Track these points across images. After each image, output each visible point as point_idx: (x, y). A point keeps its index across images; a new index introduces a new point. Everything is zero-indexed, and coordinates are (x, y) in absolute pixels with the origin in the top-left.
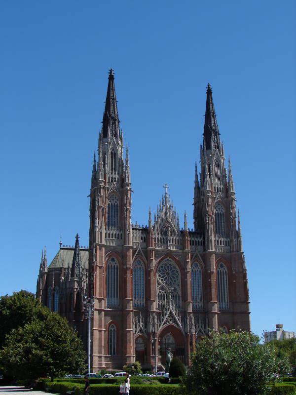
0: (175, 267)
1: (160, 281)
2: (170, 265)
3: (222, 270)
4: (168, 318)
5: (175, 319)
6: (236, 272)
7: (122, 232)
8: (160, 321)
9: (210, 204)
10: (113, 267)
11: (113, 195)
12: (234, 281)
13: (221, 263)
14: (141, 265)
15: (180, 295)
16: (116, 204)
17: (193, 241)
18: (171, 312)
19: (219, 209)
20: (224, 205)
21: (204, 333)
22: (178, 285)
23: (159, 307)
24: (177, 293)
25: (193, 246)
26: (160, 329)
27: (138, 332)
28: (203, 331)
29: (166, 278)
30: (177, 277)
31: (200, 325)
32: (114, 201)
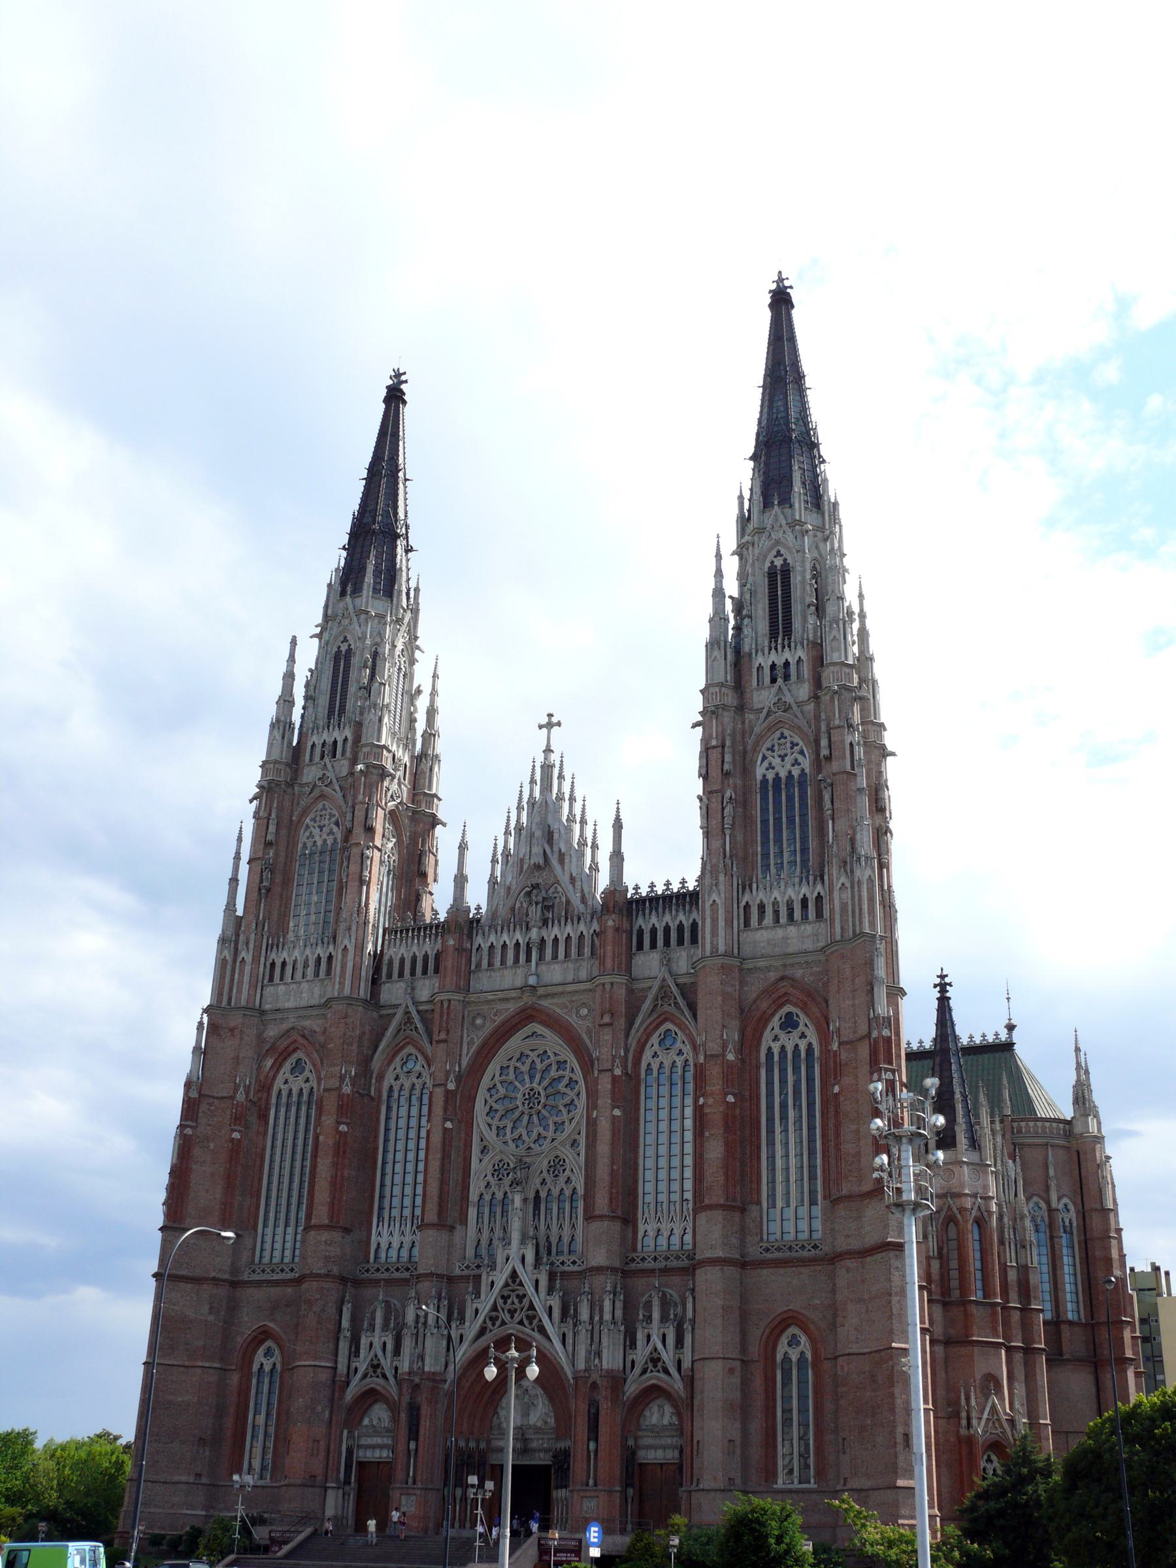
0: (561, 1064)
1: (491, 1136)
3: (789, 1041)
4: (500, 1301)
5: (532, 1307)
6: (840, 1044)
7: (331, 947)
8: (462, 1320)
9: (714, 743)
11: (324, 808)
12: (836, 1089)
13: (788, 1008)
14: (419, 1076)
15: (581, 1191)
16: (330, 842)
17: (654, 931)
18: (514, 1275)
19: (783, 757)
20: (803, 736)
21: (673, 1371)
22: (574, 1143)
23: (477, 1255)
24: (568, 1180)
27: (365, 1376)
28: (668, 1357)
29: (523, 1113)
31: (655, 1330)
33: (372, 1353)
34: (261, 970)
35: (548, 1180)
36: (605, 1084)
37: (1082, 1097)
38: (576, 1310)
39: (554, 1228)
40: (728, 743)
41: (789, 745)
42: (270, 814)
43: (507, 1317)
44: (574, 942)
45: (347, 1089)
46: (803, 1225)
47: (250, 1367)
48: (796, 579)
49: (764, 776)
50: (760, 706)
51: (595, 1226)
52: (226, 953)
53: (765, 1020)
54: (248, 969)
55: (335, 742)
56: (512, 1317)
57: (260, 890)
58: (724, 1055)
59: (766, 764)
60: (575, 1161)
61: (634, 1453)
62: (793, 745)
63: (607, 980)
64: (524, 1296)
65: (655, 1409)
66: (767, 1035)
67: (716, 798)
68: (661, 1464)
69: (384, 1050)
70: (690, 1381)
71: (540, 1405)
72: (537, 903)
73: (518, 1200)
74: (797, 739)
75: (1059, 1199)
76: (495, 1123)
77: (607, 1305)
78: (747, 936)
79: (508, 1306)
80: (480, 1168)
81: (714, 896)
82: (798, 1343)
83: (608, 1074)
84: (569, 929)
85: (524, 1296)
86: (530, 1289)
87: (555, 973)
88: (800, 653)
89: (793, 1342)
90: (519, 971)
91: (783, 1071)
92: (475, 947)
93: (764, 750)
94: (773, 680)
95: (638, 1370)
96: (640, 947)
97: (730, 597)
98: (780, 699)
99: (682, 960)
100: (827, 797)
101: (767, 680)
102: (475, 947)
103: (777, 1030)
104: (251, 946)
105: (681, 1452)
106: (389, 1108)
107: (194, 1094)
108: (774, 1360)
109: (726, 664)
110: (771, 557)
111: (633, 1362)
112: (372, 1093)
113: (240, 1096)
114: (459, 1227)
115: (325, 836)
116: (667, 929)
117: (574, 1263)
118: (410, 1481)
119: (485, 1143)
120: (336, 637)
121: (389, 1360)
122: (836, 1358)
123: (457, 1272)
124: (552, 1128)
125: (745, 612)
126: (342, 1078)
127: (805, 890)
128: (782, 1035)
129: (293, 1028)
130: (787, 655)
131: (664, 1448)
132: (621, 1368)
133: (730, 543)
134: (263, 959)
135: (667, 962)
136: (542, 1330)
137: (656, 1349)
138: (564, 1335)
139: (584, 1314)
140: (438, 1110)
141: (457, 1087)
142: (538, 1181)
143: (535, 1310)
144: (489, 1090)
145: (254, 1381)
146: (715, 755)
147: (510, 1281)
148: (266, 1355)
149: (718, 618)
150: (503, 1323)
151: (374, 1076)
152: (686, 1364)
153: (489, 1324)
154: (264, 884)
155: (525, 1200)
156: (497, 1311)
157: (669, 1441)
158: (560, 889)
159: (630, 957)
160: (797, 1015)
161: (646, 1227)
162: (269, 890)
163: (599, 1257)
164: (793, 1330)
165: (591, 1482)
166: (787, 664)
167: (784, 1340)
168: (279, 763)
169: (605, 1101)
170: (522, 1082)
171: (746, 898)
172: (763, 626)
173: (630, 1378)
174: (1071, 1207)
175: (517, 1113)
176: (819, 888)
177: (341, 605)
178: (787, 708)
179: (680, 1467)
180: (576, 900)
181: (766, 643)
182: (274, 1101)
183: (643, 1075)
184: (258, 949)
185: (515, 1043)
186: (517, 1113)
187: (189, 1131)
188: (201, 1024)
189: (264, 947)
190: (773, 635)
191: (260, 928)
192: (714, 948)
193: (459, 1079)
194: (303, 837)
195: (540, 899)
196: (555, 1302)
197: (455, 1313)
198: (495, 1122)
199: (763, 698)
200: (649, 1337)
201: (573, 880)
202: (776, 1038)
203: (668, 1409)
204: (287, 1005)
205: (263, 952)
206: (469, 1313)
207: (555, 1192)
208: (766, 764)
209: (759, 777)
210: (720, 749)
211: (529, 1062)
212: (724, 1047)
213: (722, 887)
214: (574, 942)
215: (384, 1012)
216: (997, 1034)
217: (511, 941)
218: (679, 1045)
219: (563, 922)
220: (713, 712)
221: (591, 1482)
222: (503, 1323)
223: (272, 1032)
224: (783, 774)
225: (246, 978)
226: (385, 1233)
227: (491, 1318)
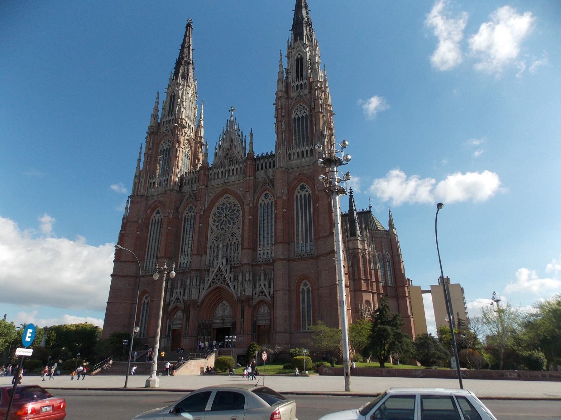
0: (235, 206)
2: (230, 203)
3: (303, 193)
4: (216, 277)
5: (225, 278)
6: (318, 191)
7: (168, 177)
8: (204, 283)
9: (279, 107)
10: (157, 221)
13: (302, 183)
15: (240, 242)
18: (220, 268)
20: (307, 104)
21: (267, 295)
22: (239, 228)
24: (237, 239)
25: (262, 171)
26: (203, 294)
27: (175, 302)
28: (266, 291)
30: (237, 217)
32: (167, 145)
33: (177, 295)
34: (147, 185)
35: (231, 239)
36: (247, 208)
37: (391, 224)
38: (238, 278)
39: (233, 254)
40: (283, 107)
41: (302, 108)
42: (150, 141)
43: (217, 281)
44: (239, 170)
45: (171, 216)
46: (308, 248)
47: (141, 302)
48: (304, 61)
49: (295, 117)
50: (292, 97)
51: (244, 251)
52: (136, 180)
53: (295, 188)
54: (143, 184)
55: (170, 120)
56: (219, 281)
57: (147, 162)
58: (282, 197)
59: (295, 114)
60: (239, 233)
61: (256, 322)
62: (303, 107)
63: (247, 178)
64: (223, 274)
65: (263, 308)
66: (296, 192)
67: (280, 124)
68: (265, 325)
69: (183, 205)
70: (273, 298)
71: (228, 309)
72: (228, 159)
73: (221, 246)
74: (305, 106)
75: (386, 252)
76: (215, 224)
77: (247, 275)
78: (290, 162)
79: (218, 278)
80: (210, 237)
81: (279, 151)
82: (307, 285)
83: (248, 206)
84: (237, 166)
85: (223, 274)
86: (224, 272)
87: (233, 179)
88: (306, 81)
89: (305, 284)
90: (223, 179)
91: (301, 202)
92: (210, 173)
93: (294, 110)
94: (297, 89)
95: (257, 295)
96: (258, 170)
97: (285, 69)
98: (299, 94)
99: (270, 171)
100: (313, 119)
101: (296, 89)
102: (210, 173)
103: (299, 190)
104: (144, 178)
105: (270, 321)
106: (185, 222)
107: (125, 221)
108: (299, 290)
109: (283, 85)
110: (297, 55)
111: (255, 293)
112: (179, 218)
113: (140, 221)
114: (204, 255)
115: (167, 146)
116: (266, 164)
117: (238, 264)
118: (187, 334)
119: (212, 230)
120: (171, 91)
121: (182, 297)
122: (318, 289)
123: (203, 268)
124: (232, 224)
125: (289, 71)
126: (169, 213)
127: (307, 148)
128: (301, 191)
129: (156, 201)
130: (301, 82)
131: (265, 320)
132: (252, 295)
133: (285, 53)
134: (148, 182)
135: (266, 173)
136: (228, 285)
137: (262, 289)
138: (234, 286)
139: (240, 279)
140: (197, 221)
141: (204, 214)
142: (228, 240)
143: (226, 279)
144: (214, 215)
145: (142, 306)
146: (279, 111)
147: (218, 270)
148: (146, 298)
149: (281, 72)
150: (216, 283)
151: (180, 213)
152: (272, 293)
153: (212, 284)
154: (148, 160)
155: (224, 246)
156: (214, 280)
157: (267, 318)
158: (235, 155)
159: (255, 172)
160: (305, 185)
161: (260, 251)
162: (150, 162)
163: (245, 261)
164: (305, 281)
165: (242, 332)
166: (301, 85)
167: (302, 284)
168: (153, 126)
169: (247, 214)
170: (224, 212)
171: (289, 152)
172: (294, 75)
173: (254, 298)
174: (389, 254)
175: (222, 221)
176: (311, 147)
177: (172, 82)
178: (301, 97)
179: (270, 326)
180: (239, 158)
181: (295, 79)
182: (151, 222)
183: (259, 207)
184: (146, 179)
185: (222, 200)
186: (222, 221)
187: (123, 232)
188: (128, 201)
189: (148, 178)
190: (297, 76)
191: (147, 173)
192: (280, 166)
193: (204, 211)
194: (161, 147)
195: (228, 158)
196: (232, 276)
197: (202, 281)
198: (215, 224)
199: (294, 94)
200: (260, 285)
201: (238, 152)
202: (299, 193)
203: (266, 308)
204: (154, 194)
205: (148, 180)
206: (206, 280)
207: (233, 243)
208: (295, 114)
209: (293, 118)
210: (281, 109)
211: (225, 205)
212: (282, 194)
213: (282, 148)
214: (239, 170)
215: (183, 194)
216: (366, 209)
217: (220, 171)
218: (270, 197)
219: (235, 164)
220: (279, 99)
221: (242, 332)
222: (216, 283)
223: (150, 202)
224: (300, 116)
225: (142, 187)
226: (183, 259)
227: (212, 282)
